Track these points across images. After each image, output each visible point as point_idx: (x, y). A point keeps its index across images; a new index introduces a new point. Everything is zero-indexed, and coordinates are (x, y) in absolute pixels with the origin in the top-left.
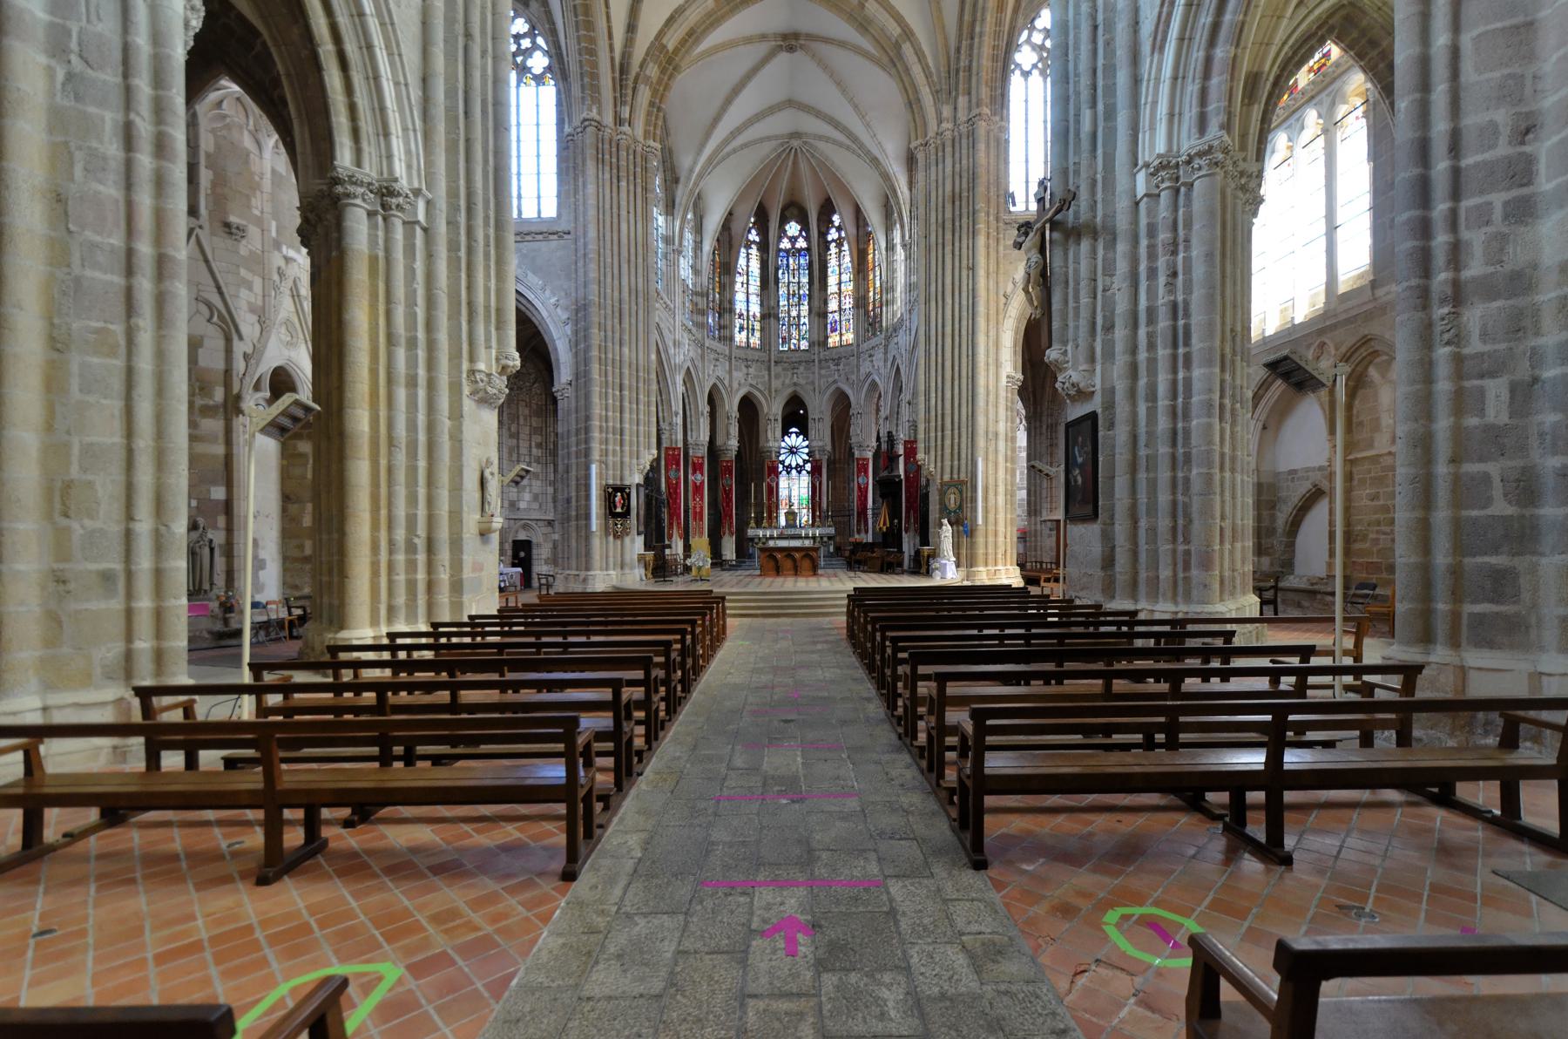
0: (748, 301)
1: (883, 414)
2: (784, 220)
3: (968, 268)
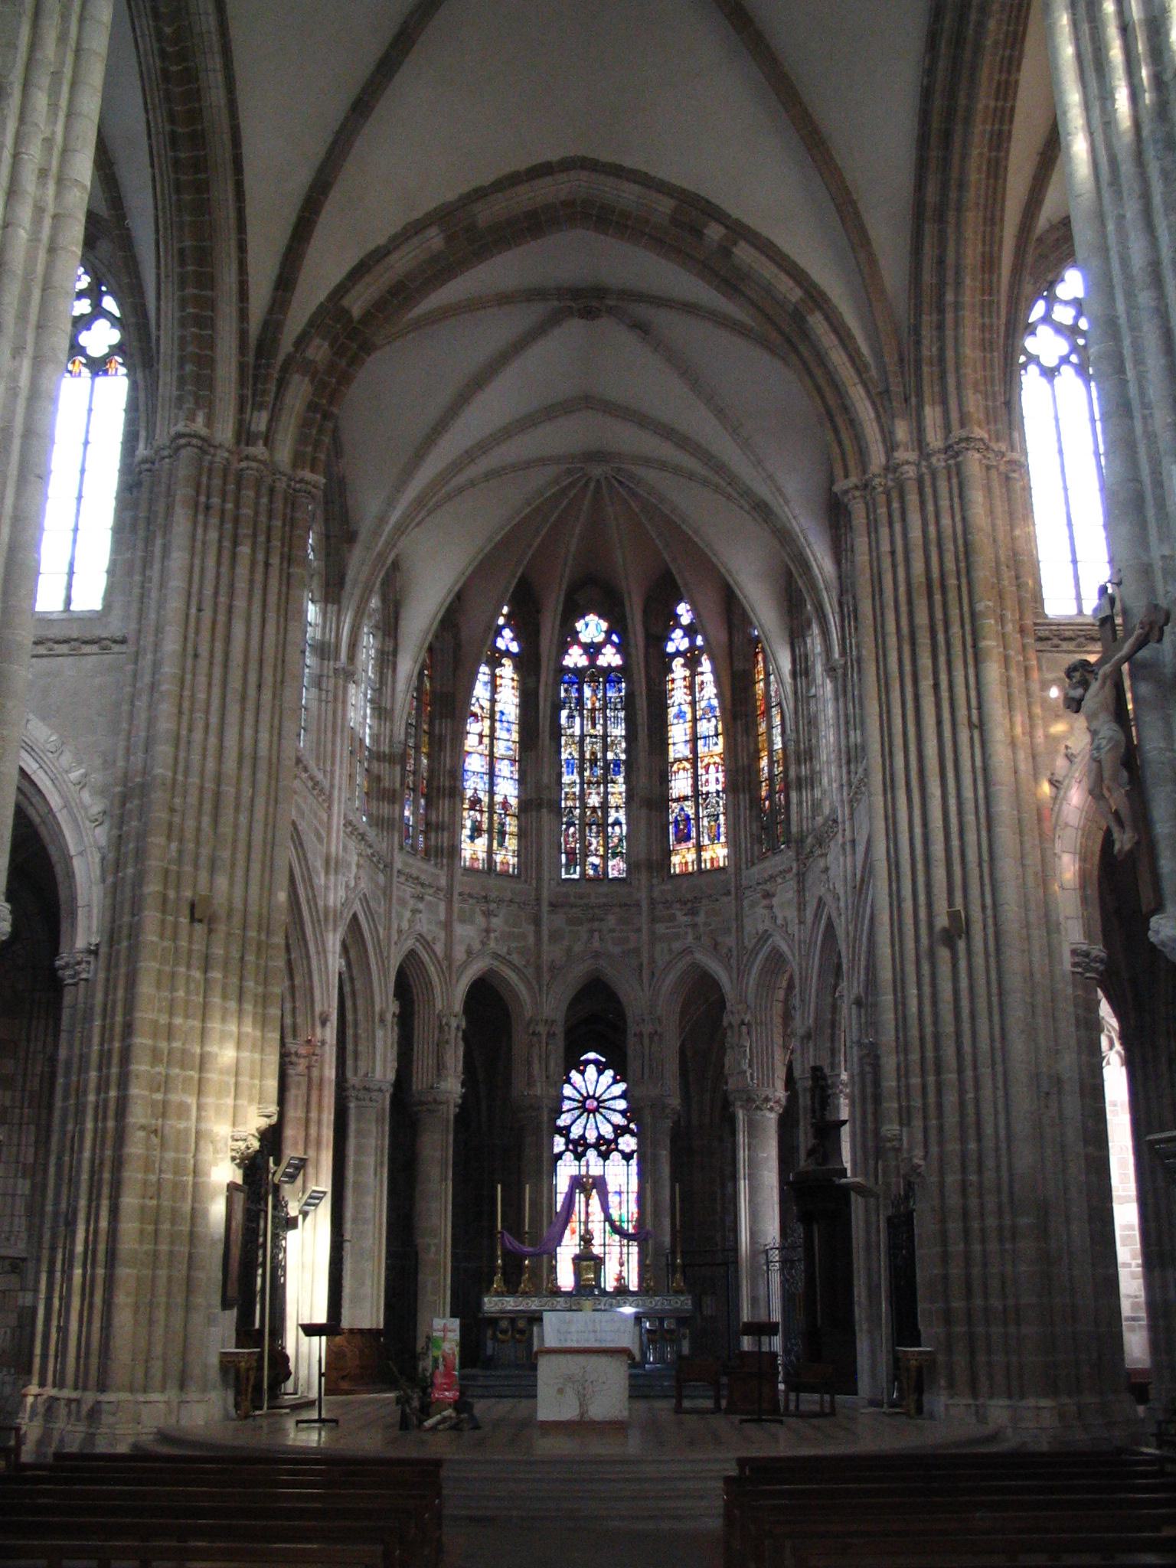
0: (492, 774)
1: (799, 1026)
2: (574, 611)
3: (971, 725)
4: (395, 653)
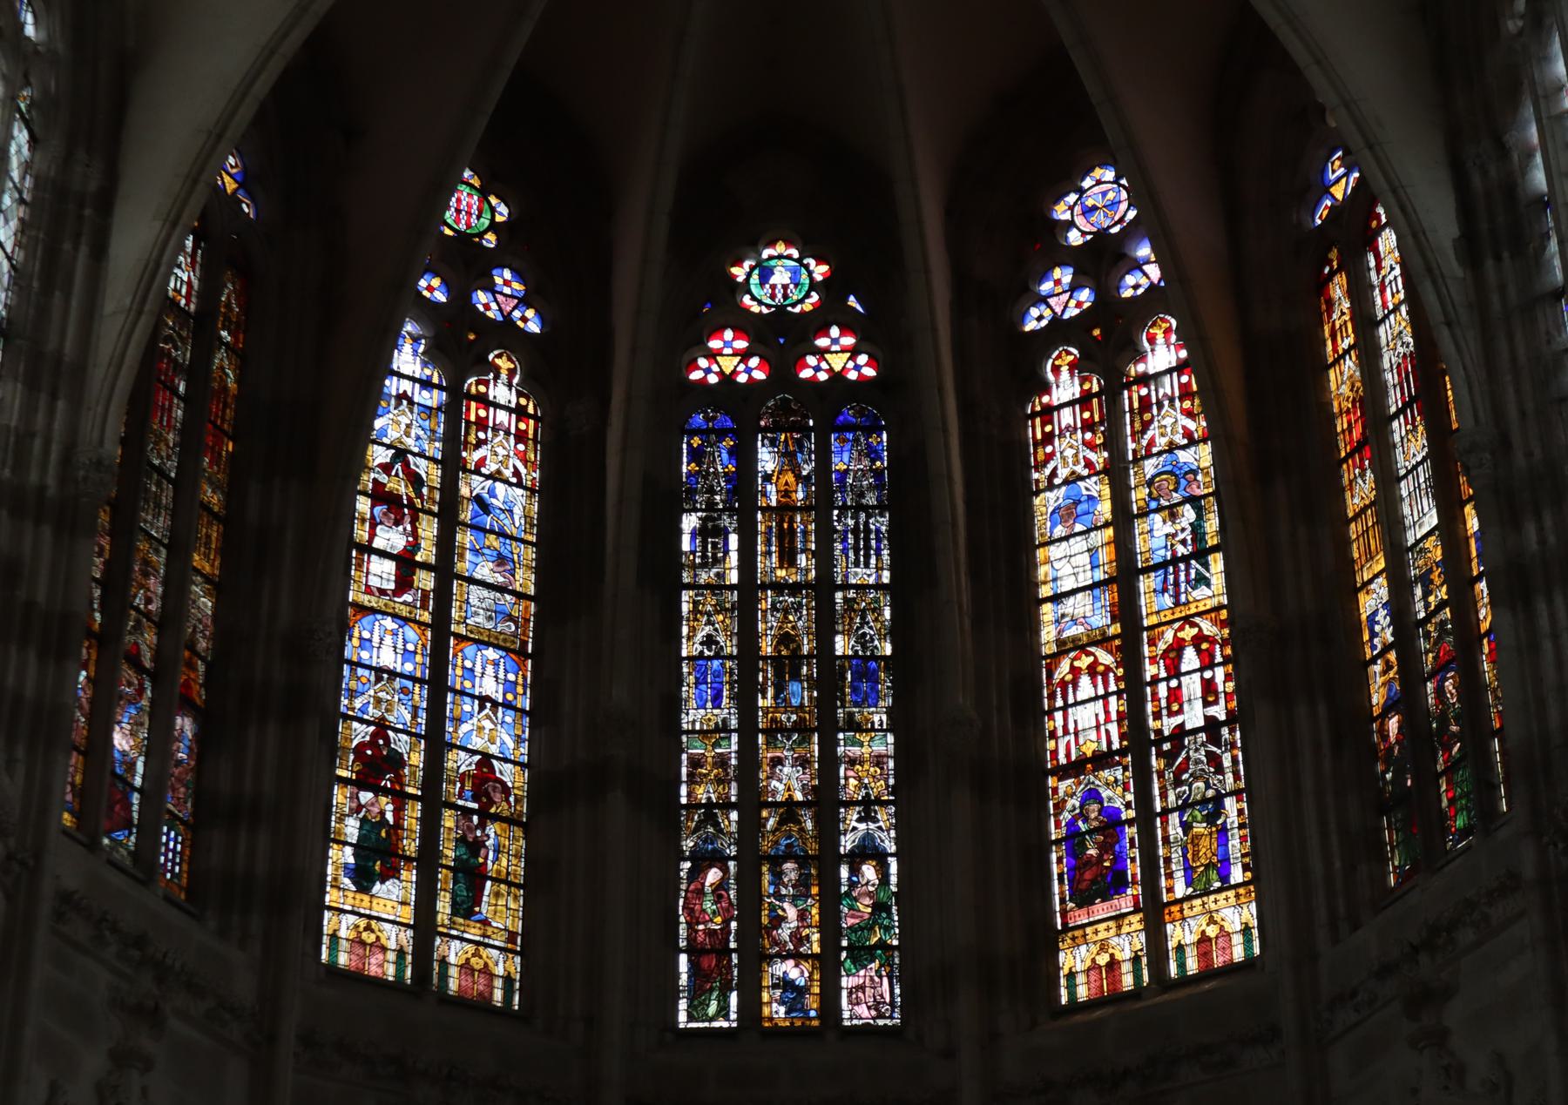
0: (437, 683)
4: (106, 201)
